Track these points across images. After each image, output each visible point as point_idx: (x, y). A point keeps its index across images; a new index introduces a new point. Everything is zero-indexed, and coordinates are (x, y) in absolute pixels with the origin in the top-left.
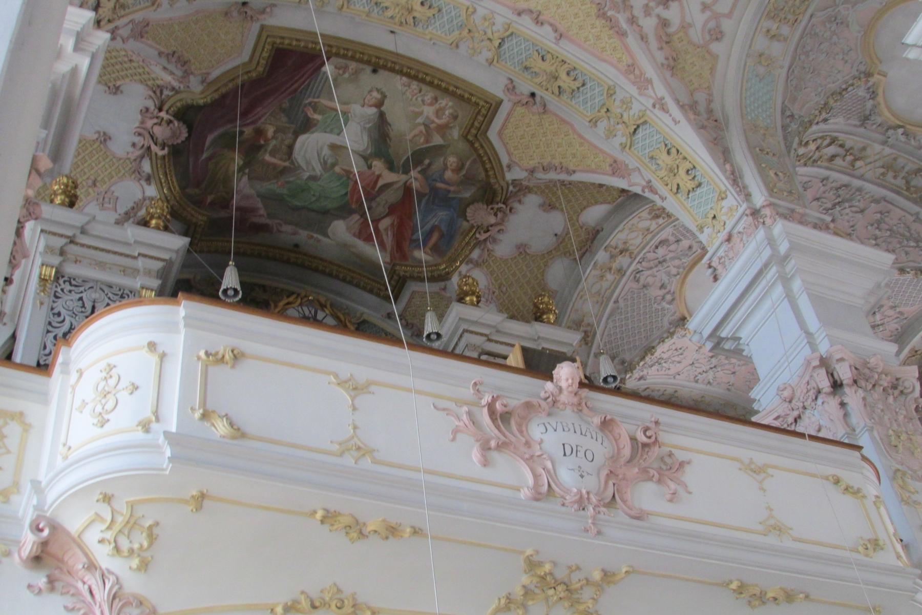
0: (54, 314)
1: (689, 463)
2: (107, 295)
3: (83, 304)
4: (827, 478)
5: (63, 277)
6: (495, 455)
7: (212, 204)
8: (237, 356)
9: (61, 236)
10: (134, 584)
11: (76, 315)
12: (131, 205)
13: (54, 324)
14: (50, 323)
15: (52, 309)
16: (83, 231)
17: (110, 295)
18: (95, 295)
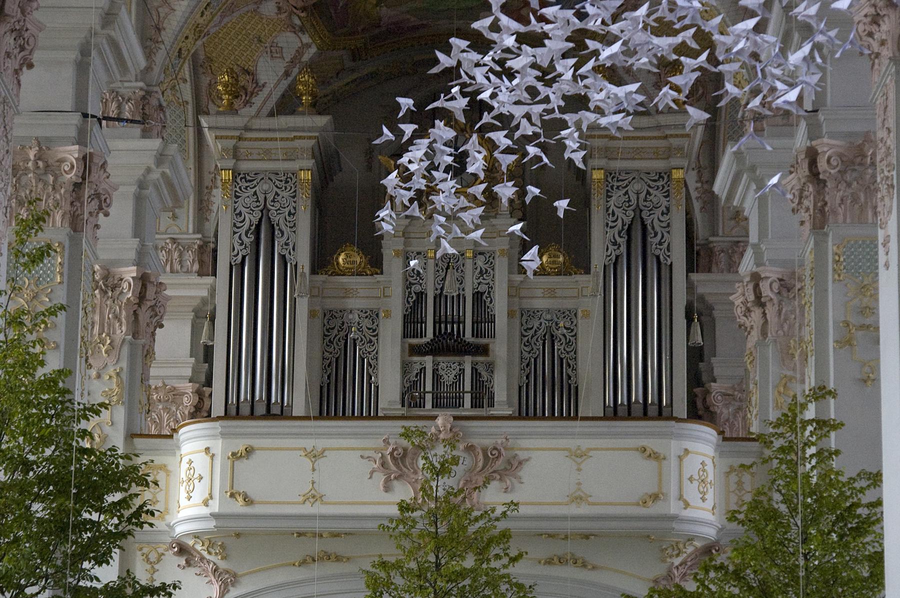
0: (236, 215)
1: (527, 460)
2: (274, 183)
3: (258, 197)
4: (637, 450)
5: (239, 174)
6: (395, 483)
7: (363, 30)
8: (249, 451)
9: (232, 137)
10: (222, 565)
11: (253, 211)
12: (293, 52)
13: (239, 225)
14: (235, 225)
15: (235, 210)
16: (247, 129)
17: (277, 183)
18: (266, 187)
